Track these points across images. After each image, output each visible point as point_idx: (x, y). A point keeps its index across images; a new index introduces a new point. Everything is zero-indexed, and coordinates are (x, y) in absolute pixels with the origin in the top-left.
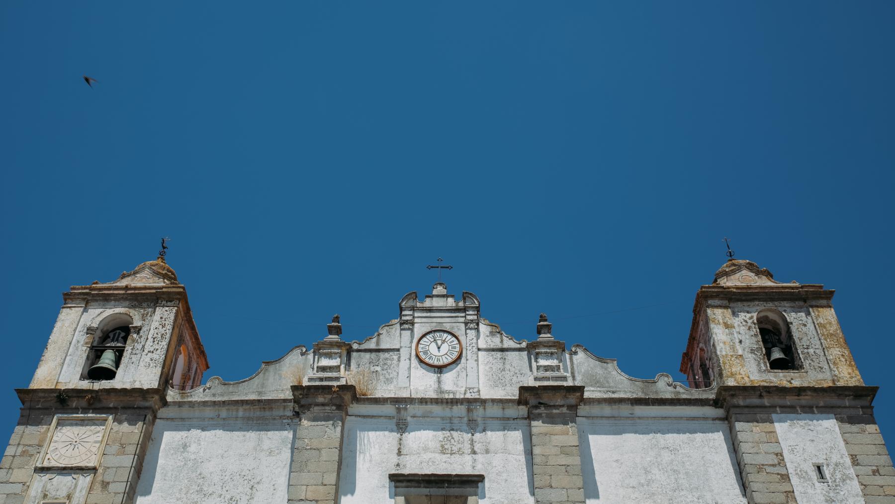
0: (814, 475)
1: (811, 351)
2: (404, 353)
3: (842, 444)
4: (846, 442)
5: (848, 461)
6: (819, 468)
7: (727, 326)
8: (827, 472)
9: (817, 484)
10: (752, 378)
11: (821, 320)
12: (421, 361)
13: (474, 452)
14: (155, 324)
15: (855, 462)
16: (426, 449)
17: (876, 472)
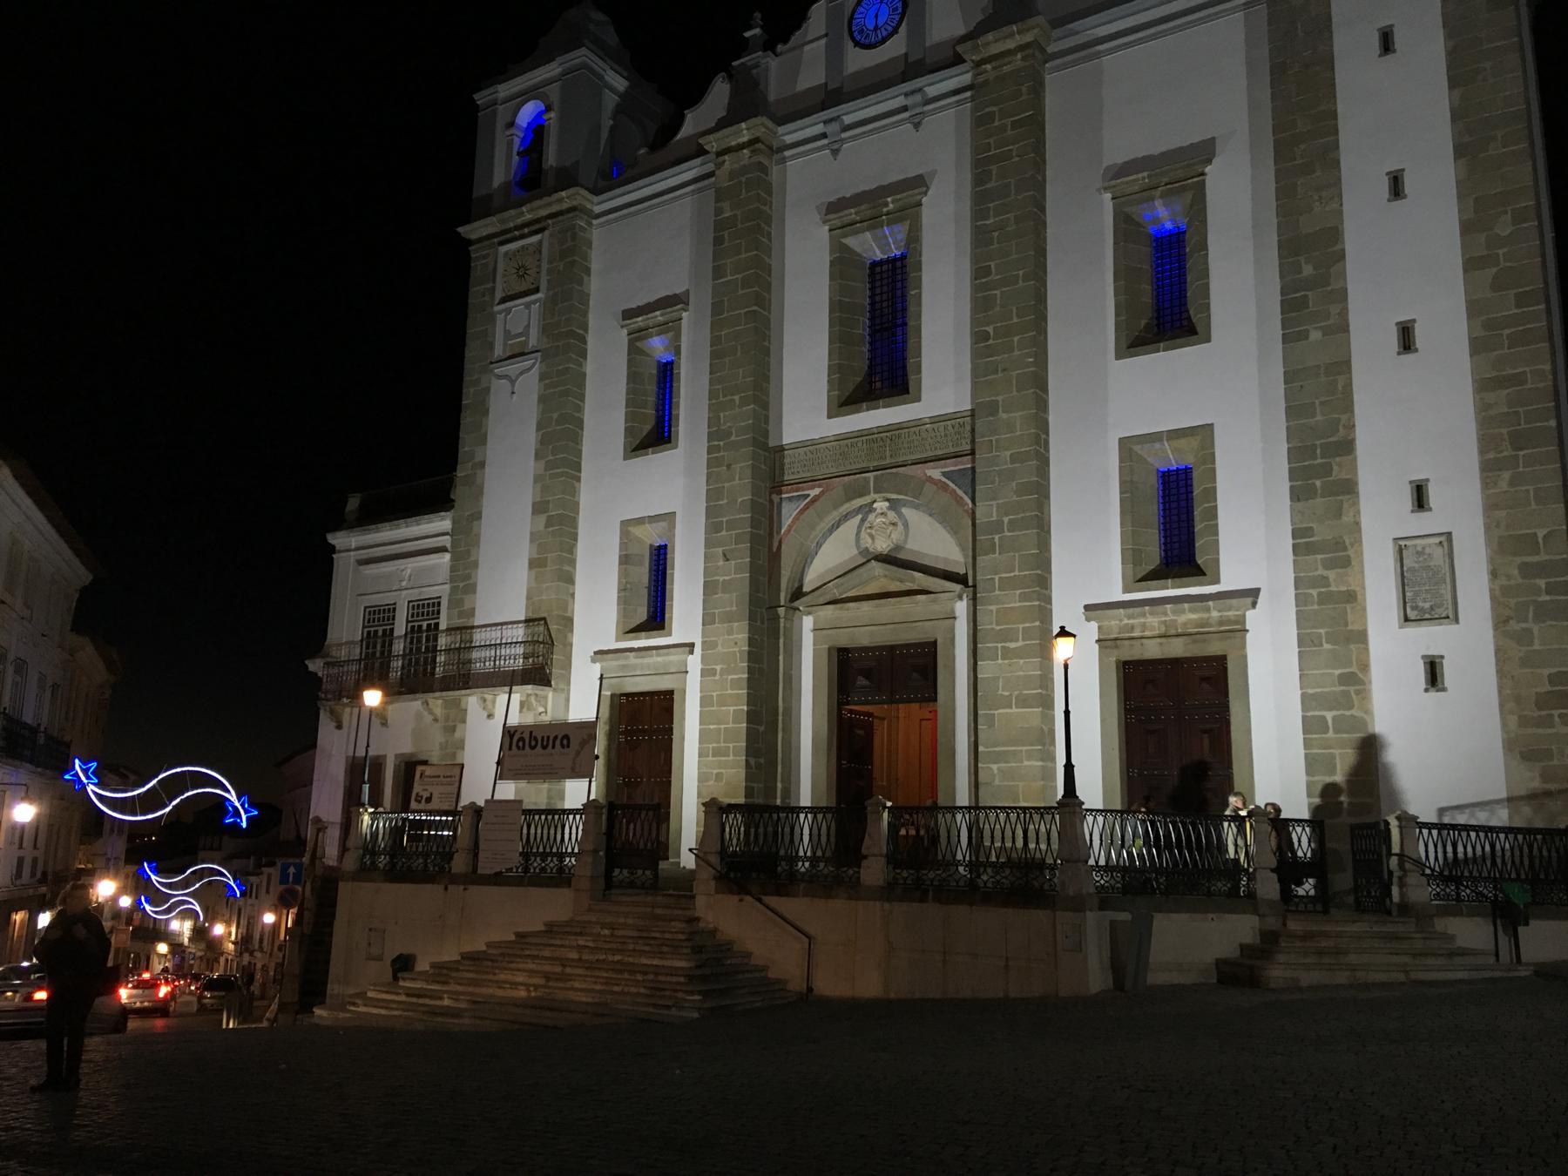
12: (857, 44)
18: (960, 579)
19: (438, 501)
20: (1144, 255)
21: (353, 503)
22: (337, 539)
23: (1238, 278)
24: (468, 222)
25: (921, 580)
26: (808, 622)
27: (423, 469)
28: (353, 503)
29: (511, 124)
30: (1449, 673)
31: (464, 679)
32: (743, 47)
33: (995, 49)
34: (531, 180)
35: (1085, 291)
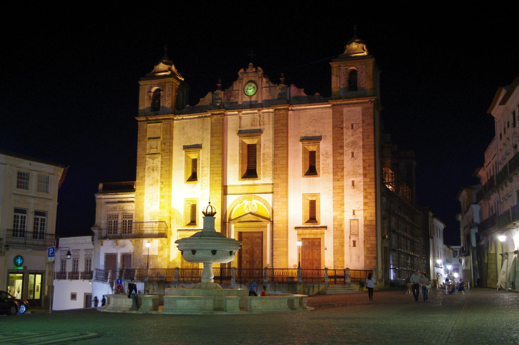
0: (350, 127)
1: (361, 83)
2: (240, 92)
3: (361, 117)
4: (363, 116)
5: (361, 121)
6: (352, 126)
7: (337, 76)
8: (354, 126)
9: (351, 130)
10: (341, 95)
11: (367, 71)
13: (260, 125)
14: (167, 91)
15: (363, 121)
16: (247, 125)
17: (368, 125)
18: (269, 219)
19: (131, 189)
20: (308, 156)
21: (101, 186)
22: (98, 196)
23: (325, 163)
24: (137, 116)
25: (260, 219)
26: (233, 226)
27: (125, 178)
28: (101, 186)
29: (150, 92)
30: (357, 243)
31: (141, 236)
32: (216, 88)
33: (278, 108)
34: (156, 107)
35: (296, 163)
